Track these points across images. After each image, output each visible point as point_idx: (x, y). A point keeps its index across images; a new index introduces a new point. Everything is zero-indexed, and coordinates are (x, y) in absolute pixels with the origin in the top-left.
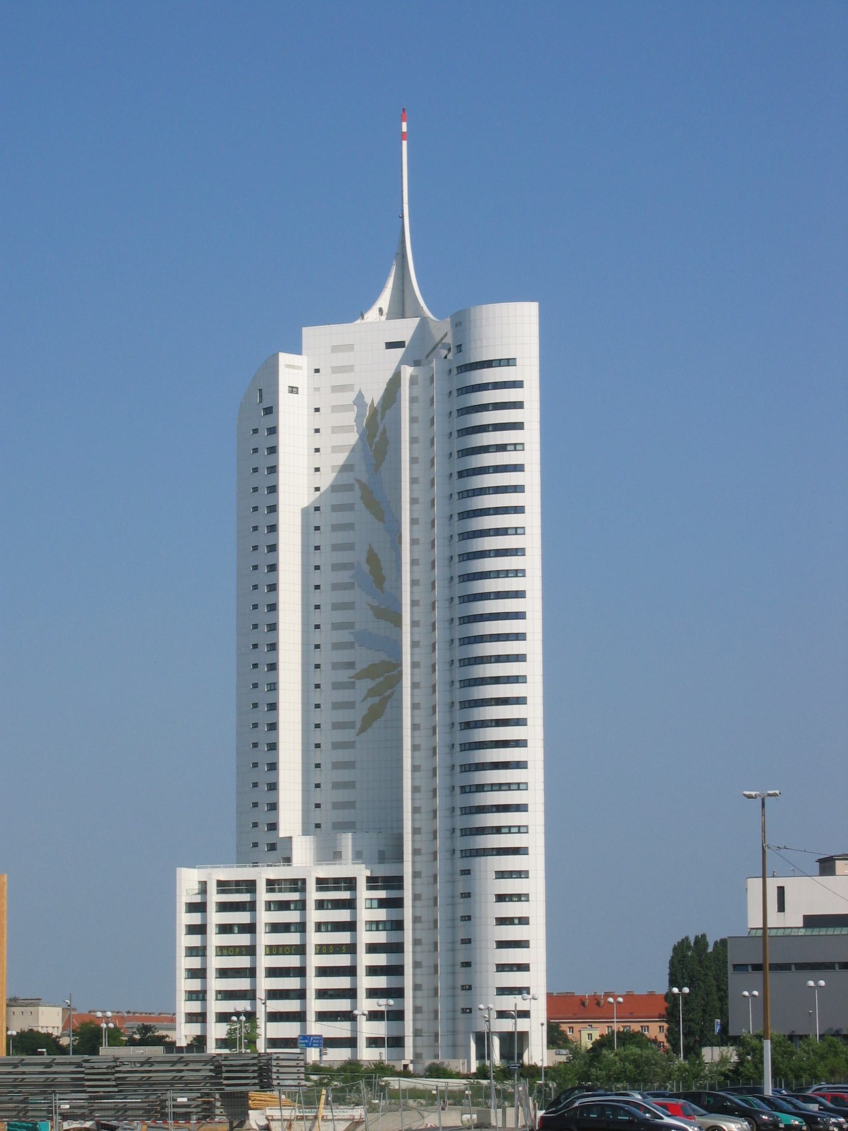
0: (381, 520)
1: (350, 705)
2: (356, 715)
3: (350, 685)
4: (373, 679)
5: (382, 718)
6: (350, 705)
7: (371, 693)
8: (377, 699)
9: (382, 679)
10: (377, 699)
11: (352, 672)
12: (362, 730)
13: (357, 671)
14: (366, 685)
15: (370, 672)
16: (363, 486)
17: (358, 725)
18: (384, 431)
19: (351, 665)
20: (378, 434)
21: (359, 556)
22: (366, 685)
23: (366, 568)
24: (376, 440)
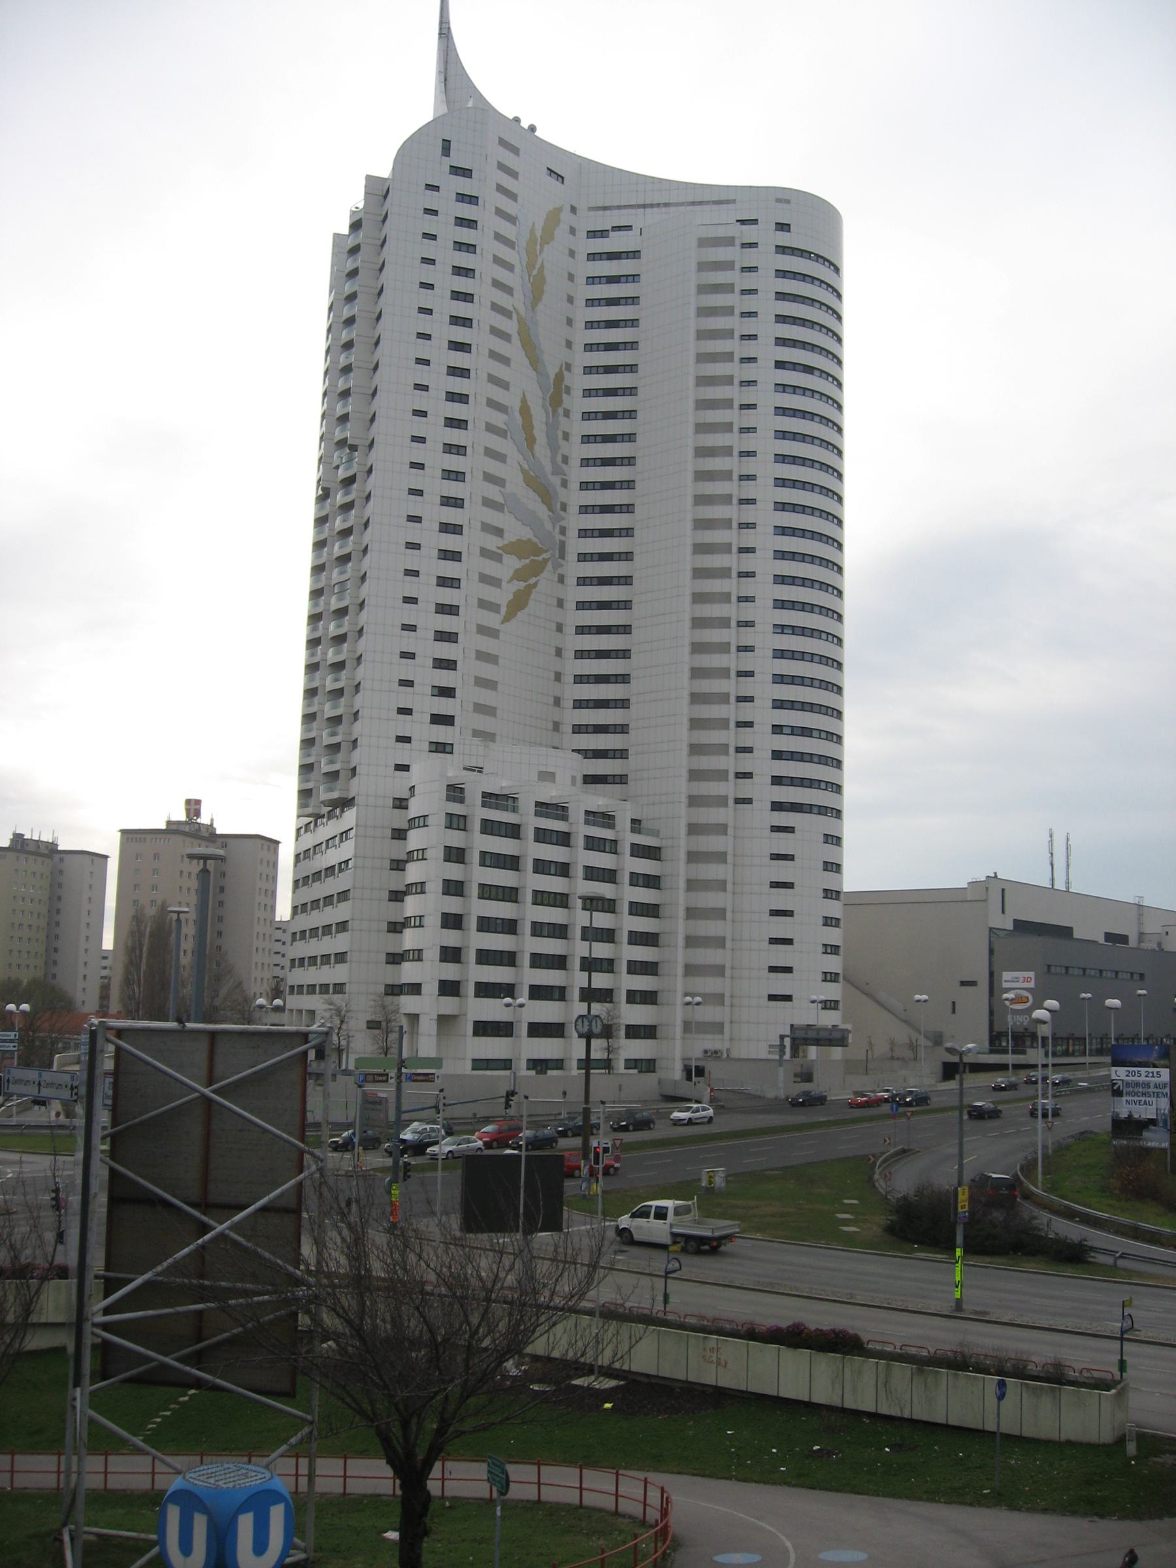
0: (535, 369)
1: (493, 581)
2: (502, 596)
3: (497, 558)
4: (520, 558)
5: (526, 610)
6: (493, 581)
7: (518, 575)
8: (523, 584)
9: (527, 561)
10: (523, 584)
11: (500, 542)
12: (506, 619)
13: (506, 542)
14: (512, 563)
15: (519, 548)
16: (520, 321)
17: (503, 610)
18: (542, 266)
19: (499, 532)
20: (537, 266)
21: (511, 399)
22: (512, 563)
23: (519, 419)
24: (535, 272)
